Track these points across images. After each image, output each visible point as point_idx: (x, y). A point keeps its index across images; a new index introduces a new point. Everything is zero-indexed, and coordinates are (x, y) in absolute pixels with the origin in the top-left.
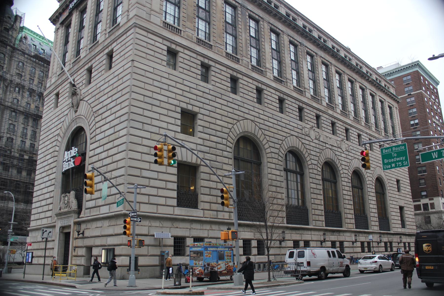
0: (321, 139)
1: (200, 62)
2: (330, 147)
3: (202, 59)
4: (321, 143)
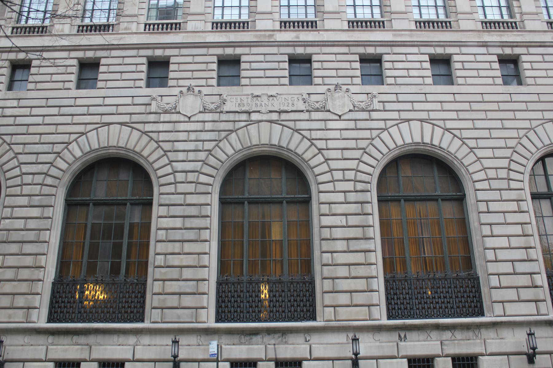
0: (226, 108)
1: (145, 58)
2: (274, 116)
3: (219, 51)
4: (224, 117)
